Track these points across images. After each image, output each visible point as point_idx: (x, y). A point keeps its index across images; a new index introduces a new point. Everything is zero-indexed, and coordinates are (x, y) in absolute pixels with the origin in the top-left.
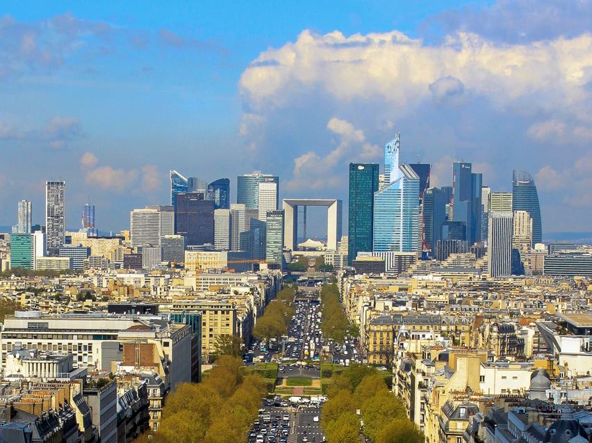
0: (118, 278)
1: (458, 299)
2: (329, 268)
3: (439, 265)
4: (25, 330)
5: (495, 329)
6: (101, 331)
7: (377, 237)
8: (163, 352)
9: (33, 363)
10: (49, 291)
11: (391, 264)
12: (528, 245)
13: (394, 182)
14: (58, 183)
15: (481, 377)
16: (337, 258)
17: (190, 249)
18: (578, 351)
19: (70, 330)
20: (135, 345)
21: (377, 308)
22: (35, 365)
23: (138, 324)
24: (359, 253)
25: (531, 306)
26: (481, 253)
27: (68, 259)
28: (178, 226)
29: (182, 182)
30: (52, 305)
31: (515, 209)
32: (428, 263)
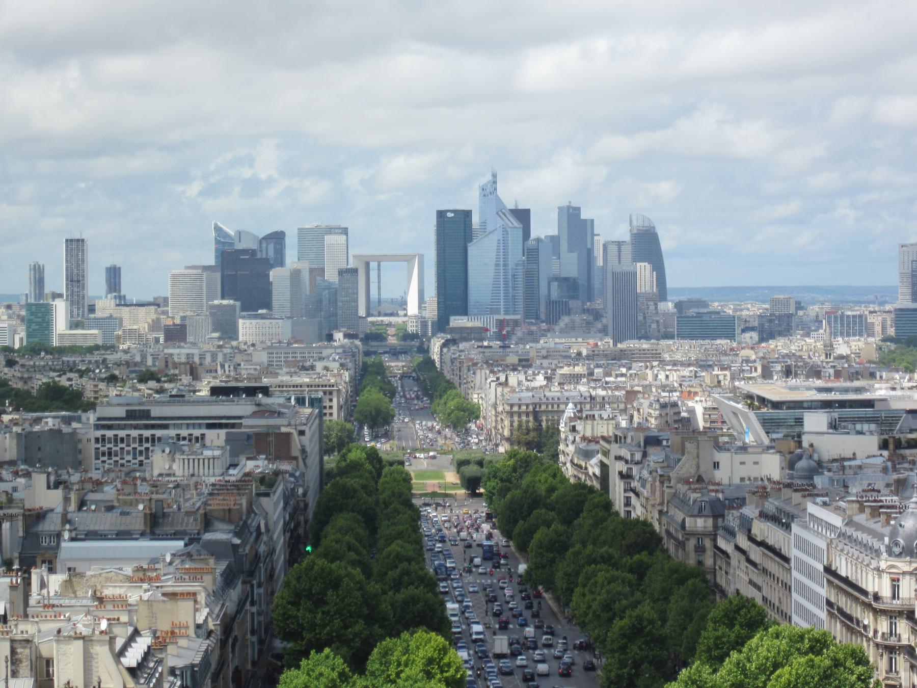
1: (596, 371)
2: (414, 336)
5: (658, 406)
9: (189, 459)
14: (78, 240)
15: (715, 463)
16: (424, 324)
17: (243, 317)
18: (824, 428)
20: (268, 434)
23: (262, 408)
24: (452, 318)
26: (597, 315)
29: (227, 235)
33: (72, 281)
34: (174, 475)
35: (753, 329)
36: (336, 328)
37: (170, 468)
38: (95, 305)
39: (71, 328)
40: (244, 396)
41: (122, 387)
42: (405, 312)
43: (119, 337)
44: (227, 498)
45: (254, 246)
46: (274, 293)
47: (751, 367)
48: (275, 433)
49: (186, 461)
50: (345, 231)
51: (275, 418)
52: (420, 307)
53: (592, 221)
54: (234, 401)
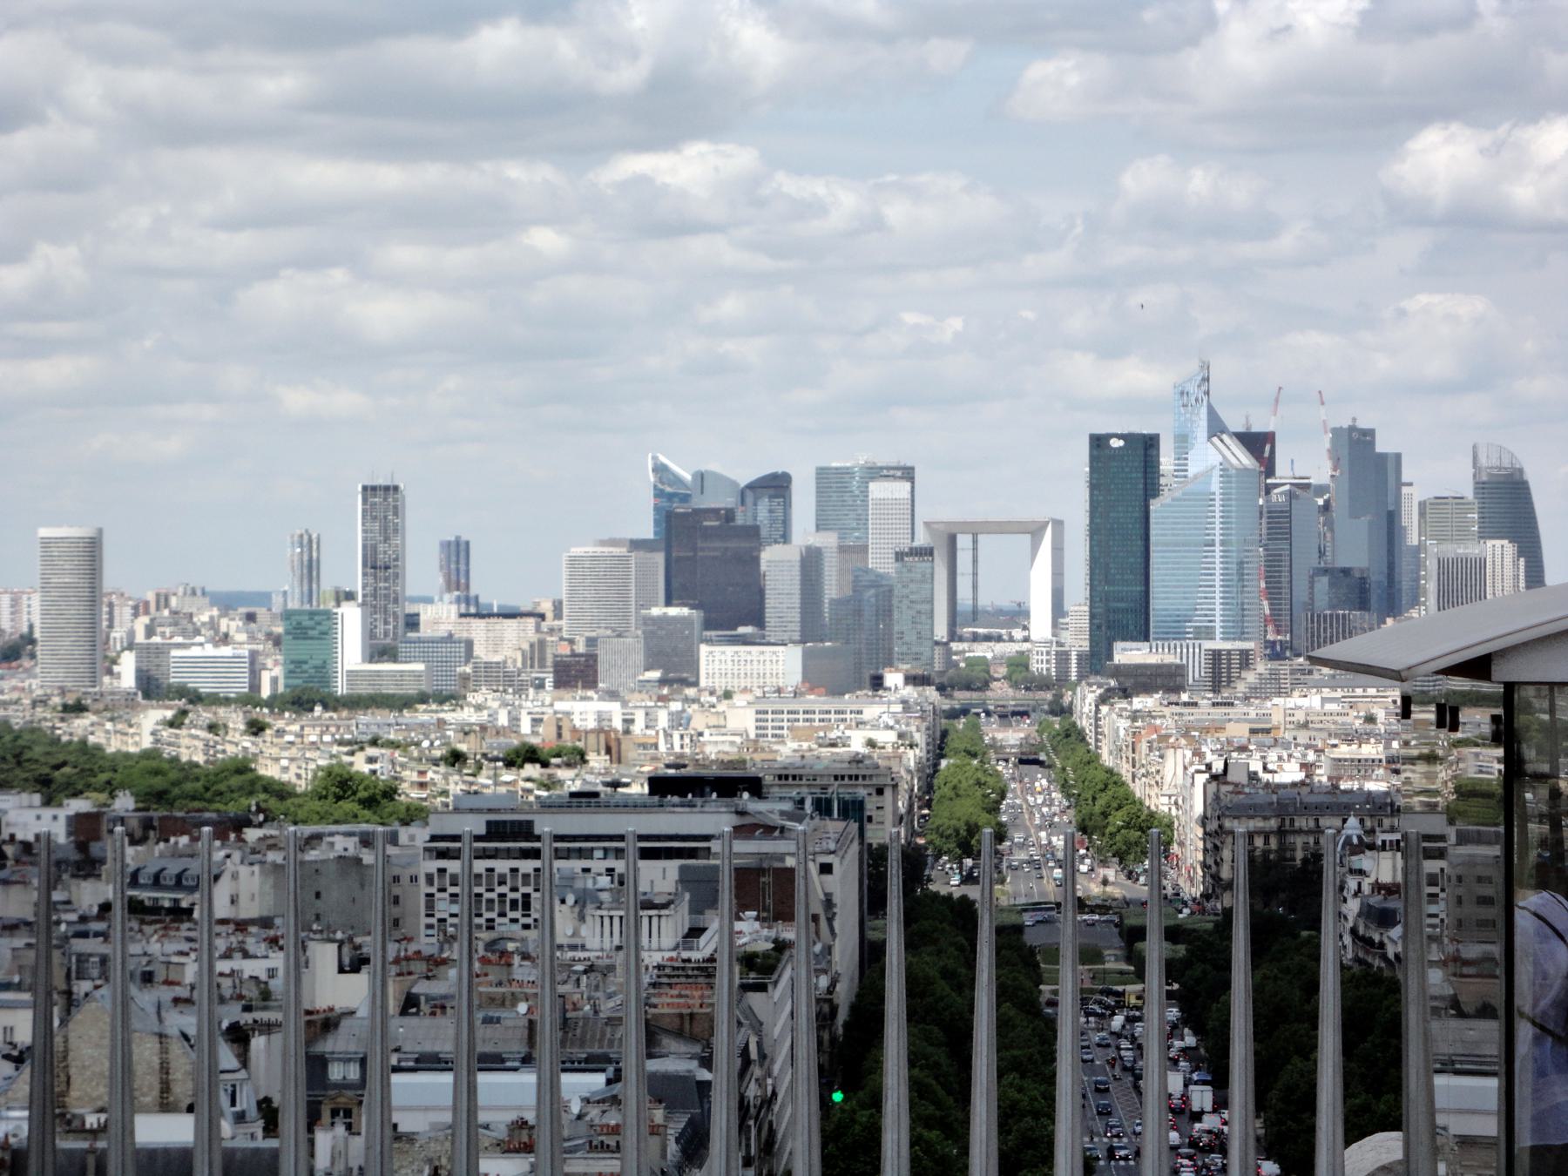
2: (1043, 684)
6: (658, 838)
7: (1162, 602)
9: (611, 917)
10: (426, 744)
11: (1197, 670)
13: (1196, 477)
14: (387, 488)
16: (1063, 658)
17: (709, 641)
19: (588, 838)
20: (760, 871)
21: (1230, 778)
22: (616, 921)
23: (747, 820)
24: (1118, 646)
27: (420, 667)
28: (675, 584)
29: (678, 480)
30: (437, 778)
31: (1485, 535)
32: (1284, 668)
33: (374, 567)
34: (583, 948)
36: (889, 663)
38: (418, 615)
39: (371, 662)
40: (714, 795)
41: (474, 775)
42: (1026, 633)
43: (465, 678)
44: (688, 992)
46: (769, 594)
48: (775, 869)
49: (607, 921)
50: (908, 474)
51: (775, 839)
52: (1055, 625)
53: (1398, 457)
54: (694, 806)
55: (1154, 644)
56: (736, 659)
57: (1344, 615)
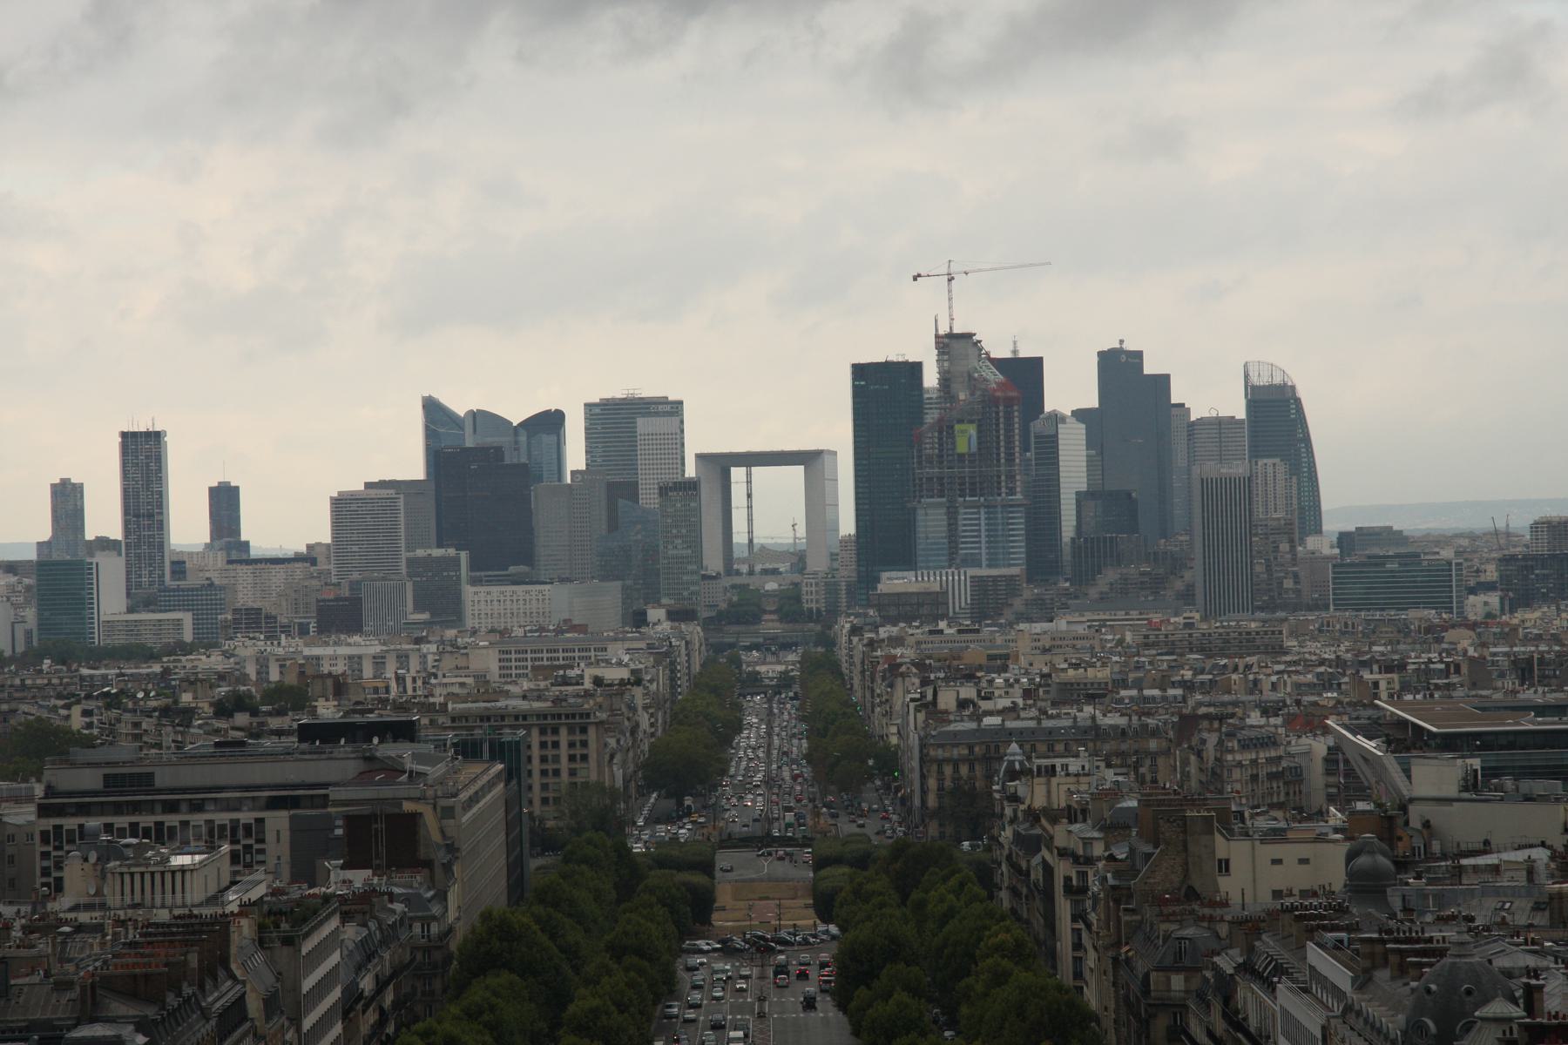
0: (306, 658)
2: (811, 616)
3: (1076, 597)
4: (95, 793)
8: (442, 832)
9: (132, 874)
10: (140, 695)
11: (961, 598)
12: (1291, 541)
16: (831, 588)
17: (475, 582)
18: (1452, 790)
20: (373, 817)
22: (137, 878)
24: (885, 575)
25: (1310, 685)
26: (1177, 564)
33: (137, 516)
34: (103, 906)
35: (1489, 587)
37: (99, 893)
45: (504, 440)
47: (1448, 664)
49: (127, 879)
50: (675, 409)
51: (401, 784)
55: (919, 573)
56: (502, 598)
57: (1111, 538)
